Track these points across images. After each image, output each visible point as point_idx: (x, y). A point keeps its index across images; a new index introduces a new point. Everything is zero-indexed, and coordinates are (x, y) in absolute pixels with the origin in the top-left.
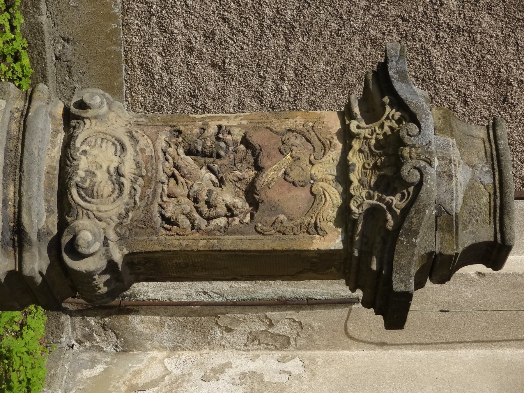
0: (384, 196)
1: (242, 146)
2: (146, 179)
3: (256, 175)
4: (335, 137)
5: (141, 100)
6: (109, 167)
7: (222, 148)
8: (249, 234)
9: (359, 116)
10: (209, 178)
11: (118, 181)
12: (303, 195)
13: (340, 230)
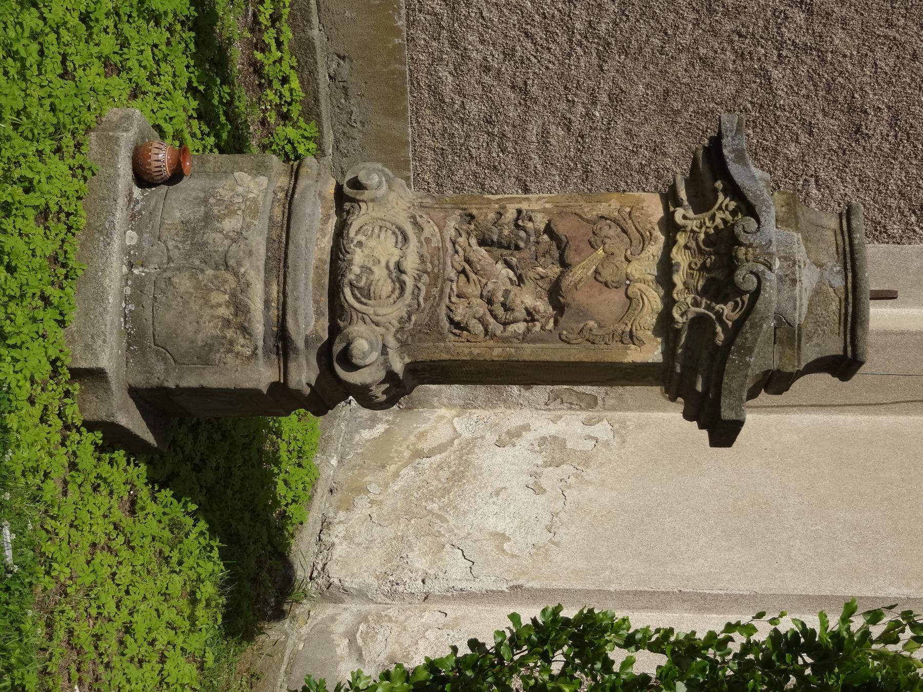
0: (714, 304)
1: (545, 237)
2: (431, 275)
3: (562, 272)
4: (657, 228)
5: (429, 126)
7: (521, 238)
8: (552, 342)
9: (686, 203)
10: (505, 274)
11: (398, 278)
12: (617, 298)
13: (659, 340)
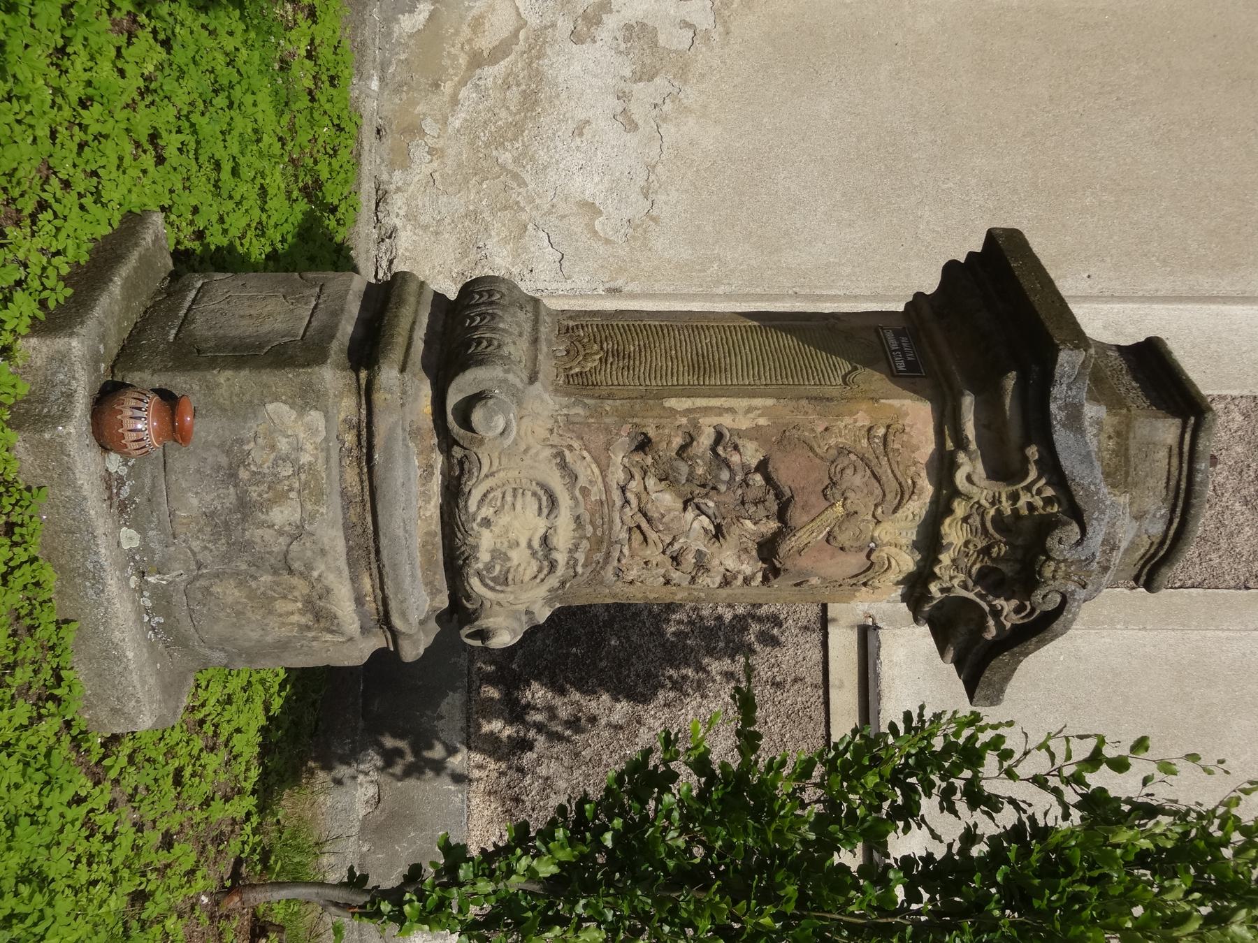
0: (991, 597)
1: (758, 478)
4: (924, 474)
6: (530, 540)
9: (973, 446)
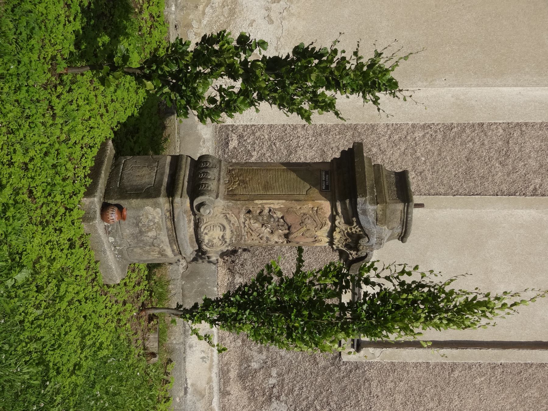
4: (328, 220)
9: (340, 214)
